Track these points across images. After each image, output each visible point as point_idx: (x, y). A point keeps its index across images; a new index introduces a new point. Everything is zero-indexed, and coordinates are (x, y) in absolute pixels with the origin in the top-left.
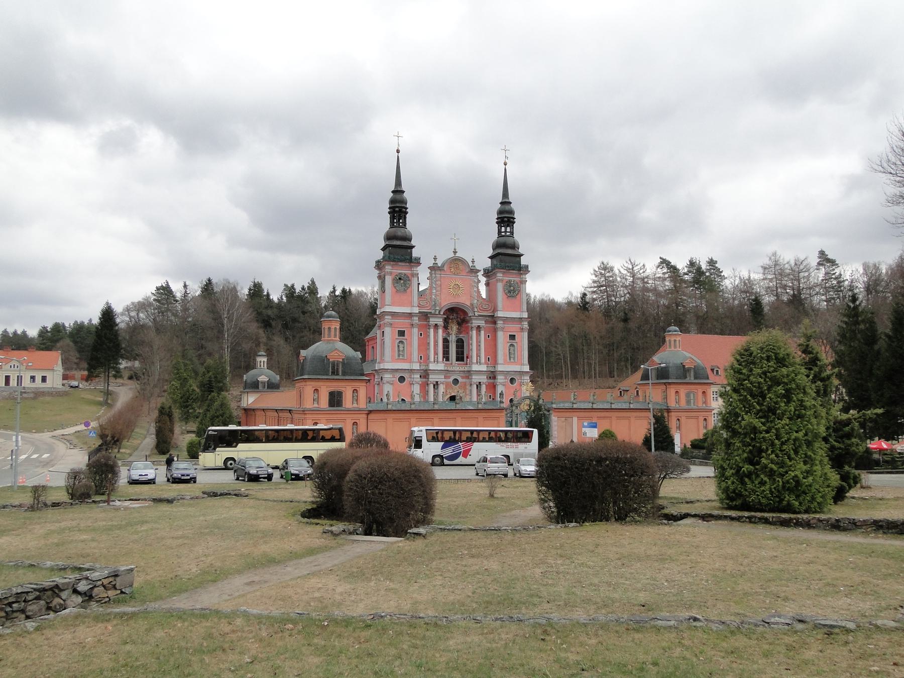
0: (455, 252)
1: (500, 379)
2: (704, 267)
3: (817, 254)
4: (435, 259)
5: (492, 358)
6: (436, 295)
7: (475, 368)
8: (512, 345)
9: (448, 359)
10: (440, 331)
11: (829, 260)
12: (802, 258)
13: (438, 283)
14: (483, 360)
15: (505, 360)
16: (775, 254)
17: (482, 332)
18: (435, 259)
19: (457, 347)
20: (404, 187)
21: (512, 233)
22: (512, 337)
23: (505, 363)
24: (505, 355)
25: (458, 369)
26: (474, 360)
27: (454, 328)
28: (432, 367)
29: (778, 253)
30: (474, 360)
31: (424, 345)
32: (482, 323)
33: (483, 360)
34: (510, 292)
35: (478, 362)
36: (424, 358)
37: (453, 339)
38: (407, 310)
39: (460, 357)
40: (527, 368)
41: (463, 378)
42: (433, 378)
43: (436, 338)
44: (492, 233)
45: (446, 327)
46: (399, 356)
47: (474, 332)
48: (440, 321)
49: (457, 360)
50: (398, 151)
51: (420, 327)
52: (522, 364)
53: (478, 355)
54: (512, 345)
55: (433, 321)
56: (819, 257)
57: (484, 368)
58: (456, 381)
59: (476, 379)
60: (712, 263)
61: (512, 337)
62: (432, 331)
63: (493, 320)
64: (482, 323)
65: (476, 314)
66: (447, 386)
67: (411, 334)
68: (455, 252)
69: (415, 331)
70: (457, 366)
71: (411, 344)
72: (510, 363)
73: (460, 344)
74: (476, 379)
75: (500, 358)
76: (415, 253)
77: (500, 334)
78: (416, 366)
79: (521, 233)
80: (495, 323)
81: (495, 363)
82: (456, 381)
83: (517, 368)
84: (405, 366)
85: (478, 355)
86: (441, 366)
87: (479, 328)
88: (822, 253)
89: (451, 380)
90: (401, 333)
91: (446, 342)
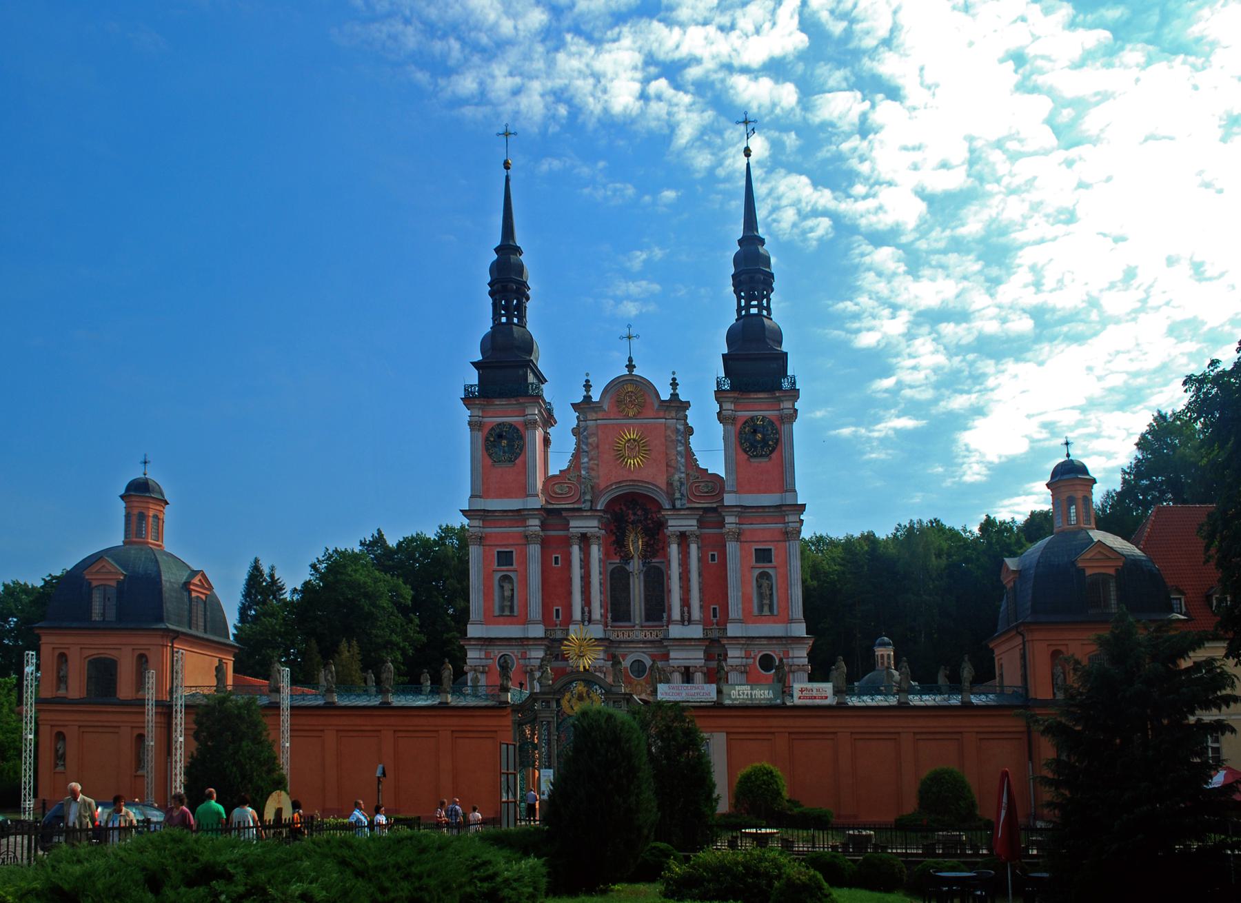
0: (631, 367)
4: (588, 386)
5: (716, 610)
6: (589, 469)
7: (675, 631)
8: (764, 575)
14: (696, 614)
17: (694, 548)
18: (588, 386)
20: (519, 240)
24: (746, 599)
25: (641, 636)
26: (676, 615)
27: (635, 544)
30: (676, 615)
31: (555, 586)
32: (689, 524)
33: (696, 614)
34: (753, 446)
35: (686, 620)
40: (800, 630)
43: (589, 567)
46: (502, 609)
47: (674, 549)
48: (590, 525)
50: (507, 166)
51: (545, 543)
52: (791, 621)
53: (685, 602)
54: (764, 575)
55: (577, 525)
57: (696, 631)
61: (763, 556)
62: (575, 550)
63: (712, 515)
64: (689, 524)
67: (524, 561)
68: (631, 367)
72: (760, 618)
75: (735, 610)
77: (732, 548)
80: (721, 524)
81: (724, 621)
83: (777, 630)
84: (514, 631)
85: (685, 602)
87: (683, 538)
90: (505, 558)
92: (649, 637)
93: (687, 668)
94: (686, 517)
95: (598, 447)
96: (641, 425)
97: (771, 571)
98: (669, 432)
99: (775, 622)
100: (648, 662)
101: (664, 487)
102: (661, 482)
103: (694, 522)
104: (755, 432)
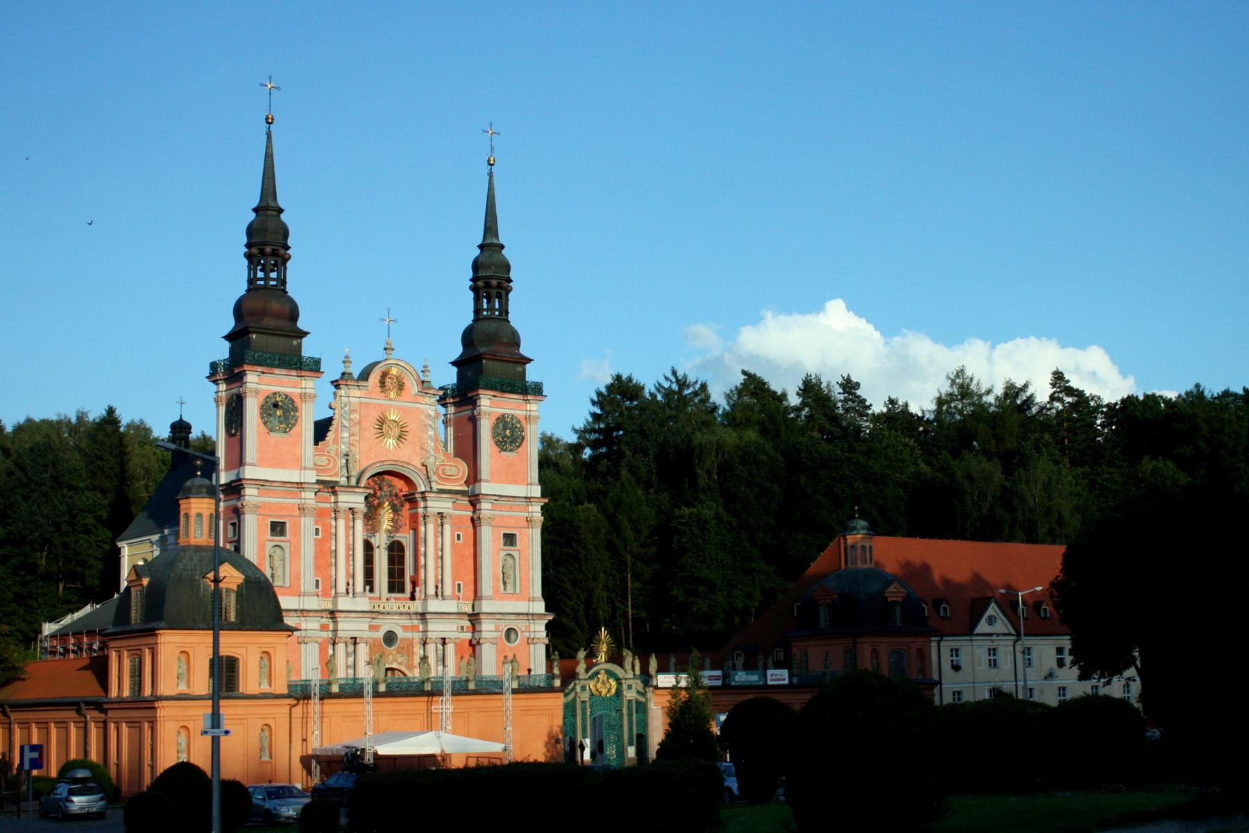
1: (488, 628)
2: (837, 393)
3: (1049, 378)
4: (346, 361)
7: (434, 605)
9: (372, 590)
10: (359, 524)
11: (1070, 391)
12: (1019, 384)
13: (356, 416)
15: (496, 591)
16: (960, 373)
17: (447, 528)
18: (346, 361)
19: (391, 560)
21: (504, 311)
22: (510, 539)
23: (496, 596)
24: (495, 579)
25: (395, 609)
28: (343, 604)
29: (968, 373)
33: (448, 591)
36: (325, 585)
37: (381, 541)
38: (293, 476)
39: (396, 585)
41: (405, 628)
42: (347, 627)
44: (461, 310)
45: (371, 516)
48: (356, 500)
49: (392, 589)
51: (320, 514)
56: (1054, 385)
58: (390, 638)
59: (437, 628)
60: (849, 386)
61: (510, 539)
62: (341, 523)
65: (435, 487)
66: (373, 646)
67: (297, 533)
69: (308, 524)
70: (397, 603)
71: (296, 553)
72: (506, 597)
73: (396, 551)
74: (437, 628)
75: (487, 587)
76: (309, 349)
77: (486, 532)
78: (312, 603)
79: (522, 312)
81: (477, 596)
82: (390, 638)
83: (522, 607)
86: (363, 603)
88: (1058, 377)
89: (380, 634)
91: (368, 547)
92: (402, 609)
93: (444, 639)
94: (443, 500)
95: (360, 423)
96: (399, 408)
97: (516, 554)
98: (422, 417)
99: (518, 599)
100: (400, 634)
101: (419, 465)
102: (417, 462)
103: (450, 505)
104: (505, 429)
